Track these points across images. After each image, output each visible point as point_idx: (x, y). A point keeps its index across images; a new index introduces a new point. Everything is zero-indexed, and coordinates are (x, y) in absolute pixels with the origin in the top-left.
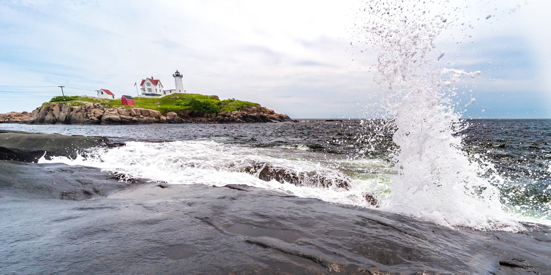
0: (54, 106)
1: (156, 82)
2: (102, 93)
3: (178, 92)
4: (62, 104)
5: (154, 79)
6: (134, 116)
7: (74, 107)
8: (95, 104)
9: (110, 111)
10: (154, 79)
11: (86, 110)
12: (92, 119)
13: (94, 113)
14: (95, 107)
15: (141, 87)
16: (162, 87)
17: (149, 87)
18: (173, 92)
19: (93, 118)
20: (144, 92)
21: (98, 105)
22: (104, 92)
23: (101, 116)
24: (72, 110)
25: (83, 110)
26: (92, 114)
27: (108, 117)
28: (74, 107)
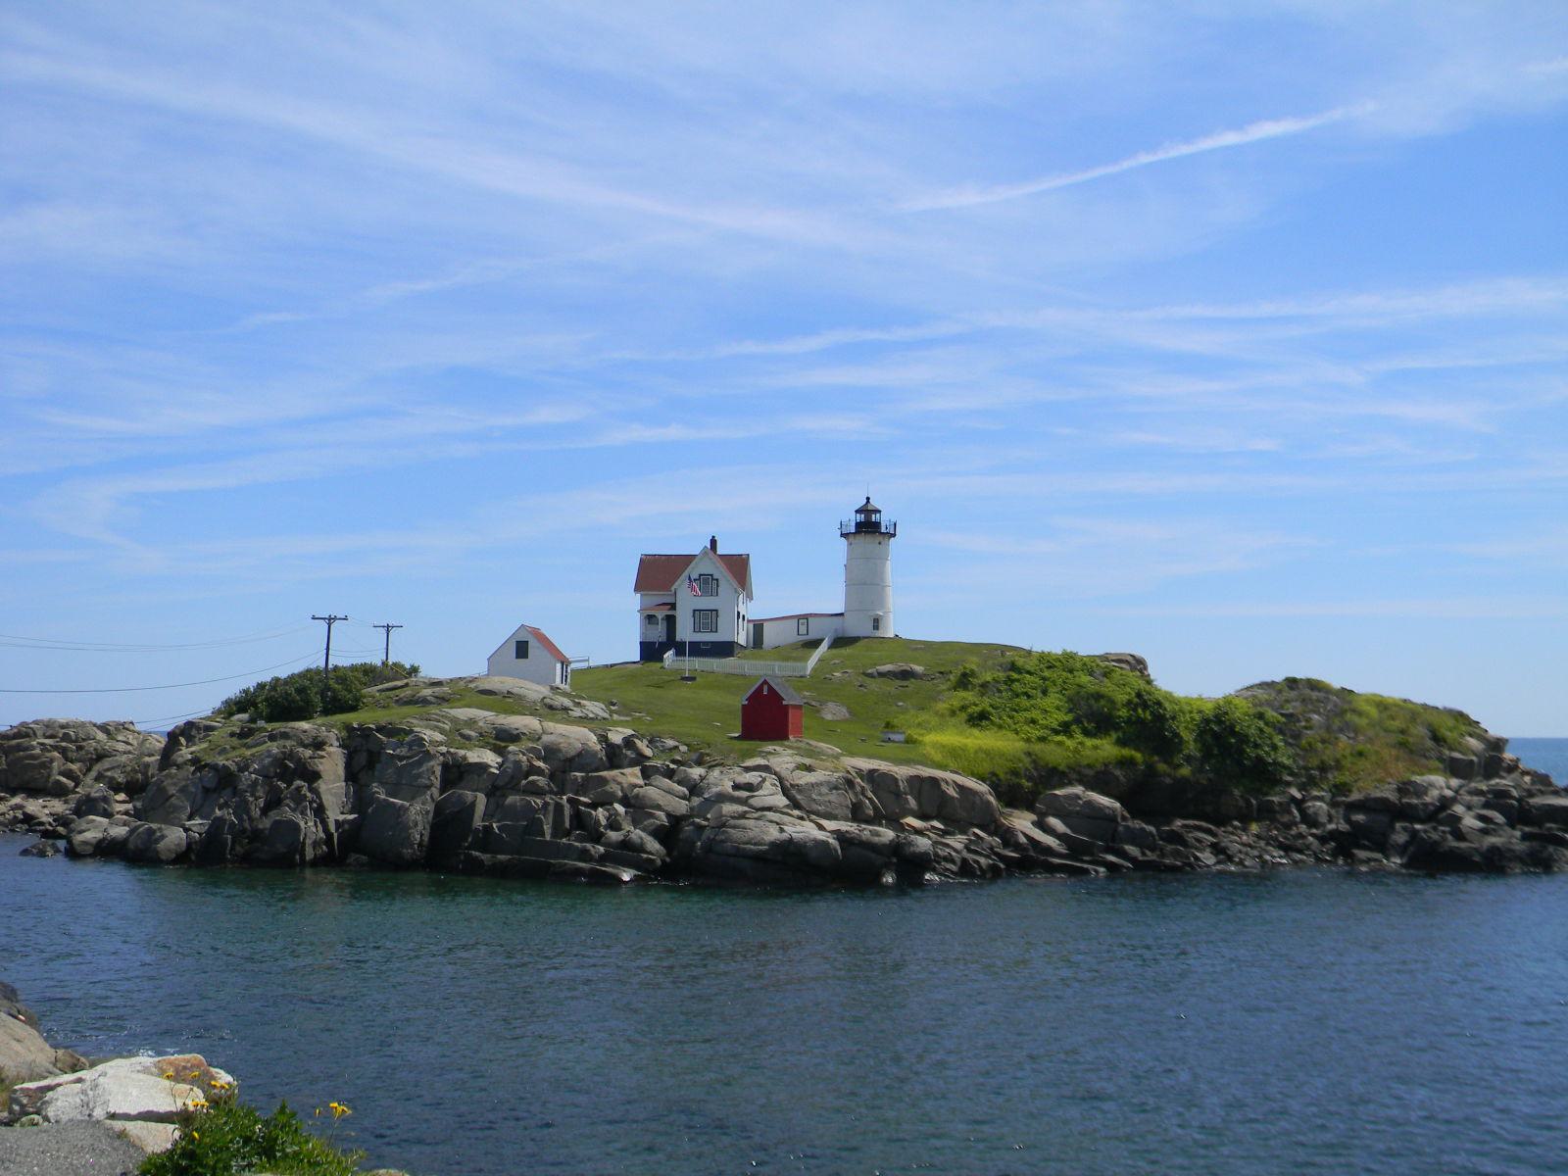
1: (738, 566)
2: (522, 650)
3: (866, 629)
4: (365, 733)
8: (616, 737)
9: (749, 787)
11: (552, 777)
12: (626, 844)
13: (625, 801)
16: (750, 597)
17: (706, 603)
19: (637, 834)
20: (658, 633)
21: (628, 742)
22: (533, 644)
26: (620, 809)
27: (773, 834)
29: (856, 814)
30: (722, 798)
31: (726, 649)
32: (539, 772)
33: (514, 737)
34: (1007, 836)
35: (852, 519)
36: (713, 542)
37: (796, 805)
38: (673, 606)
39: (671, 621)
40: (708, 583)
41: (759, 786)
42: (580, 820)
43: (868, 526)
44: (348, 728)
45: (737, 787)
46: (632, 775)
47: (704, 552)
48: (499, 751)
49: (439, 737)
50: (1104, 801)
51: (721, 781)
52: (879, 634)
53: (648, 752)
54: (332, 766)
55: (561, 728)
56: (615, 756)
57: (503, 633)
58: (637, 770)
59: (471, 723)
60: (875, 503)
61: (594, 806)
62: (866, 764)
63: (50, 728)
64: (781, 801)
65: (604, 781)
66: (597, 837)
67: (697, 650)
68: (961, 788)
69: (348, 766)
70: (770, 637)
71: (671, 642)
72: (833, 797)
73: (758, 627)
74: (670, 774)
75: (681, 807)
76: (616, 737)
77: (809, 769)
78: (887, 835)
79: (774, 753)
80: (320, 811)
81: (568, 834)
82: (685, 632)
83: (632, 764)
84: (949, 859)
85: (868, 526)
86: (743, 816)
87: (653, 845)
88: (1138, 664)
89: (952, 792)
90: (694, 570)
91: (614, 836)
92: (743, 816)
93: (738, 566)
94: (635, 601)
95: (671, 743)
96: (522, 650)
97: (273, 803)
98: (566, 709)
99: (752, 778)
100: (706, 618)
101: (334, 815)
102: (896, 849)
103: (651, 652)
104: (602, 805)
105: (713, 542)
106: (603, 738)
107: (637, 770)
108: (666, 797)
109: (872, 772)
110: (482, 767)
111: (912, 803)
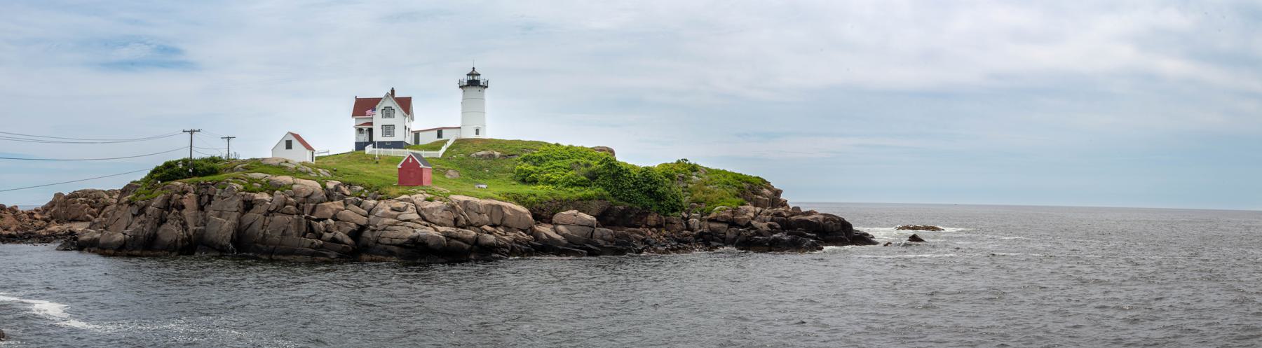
0: (184, 192)
2: (289, 145)
3: (473, 135)
4: (206, 186)
5: (397, 95)
6: (469, 225)
7: (258, 196)
9: (399, 210)
10: (397, 95)
11: (297, 206)
12: (334, 240)
13: (335, 218)
14: (330, 196)
15: (353, 122)
17: (388, 121)
18: (450, 137)
19: (340, 235)
21: (337, 188)
22: (295, 143)
23: (362, 228)
24: (249, 205)
25: (293, 208)
26: (331, 221)
27: (410, 234)
28: (258, 196)
29: (456, 223)
30: (385, 215)
31: (399, 145)
32: (291, 204)
33: (280, 186)
34: (537, 236)
35: (465, 79)
36: (393, 91)
37: (424, 219)
38: (371, 124)
39: (370, 131)
40: (388, 112)
41: (405, 209)
42: (310, 228)
43: (474, 82)
44: (198, 184)
45: (393, 210)
46: (337, 205)
47: (387, 96)
48: (271, 193)
49: (241, 187)
50: (588, 217)
51: (384, 207)
52: (481, 136)
53: (348, 193)
54: (190, 201)
55: (303, 181)
56: (330, 196)
57: (279, 136)
58: (341, 202)
59: (258, 181)
60: (477, 71)
61: (318, 220)
62: (462, 198)
63: (86, 194)
64: (416, 216)
65: (324, 208)
66: (319, 236)
67: (382, 145)
68: (514, 210)
69: (199, 201)
70: (423, 141)
71: (371, 141)
72: (444, 214)
73: (417, 134)
74: (359, 204)
75: (363, 221)
76: (331, 185)
77: (430, 200)
78: (471, 233)
79: (415, 193)
80: (184, 225)
81: (304, 235)
82: (378, 137)
83: (339, 198)
84: (505, 246)
85: (474, 82)
86: (395, 224)
87: (348, 240)
88: (612, 152)
89: (508, 212)
90: (380, 107)
91: (328, 236)
92: (395, 224)
93: (405, 104)
94: (353, 122)
95: (360, 188)
96: (289, 145)
97: (162, 221)
98: (308, 173)
99: (401, 205)
100: (388, 129)
101: (192, 227)
102: (476, 241)
103: (360, 146)
104: (323, 220)
105: (393, 91)
106: (324, 187)
107: (341, 202)
108: (354, 216)
109: (466, 202)
110: (263, 201)
111: (486, 218)
